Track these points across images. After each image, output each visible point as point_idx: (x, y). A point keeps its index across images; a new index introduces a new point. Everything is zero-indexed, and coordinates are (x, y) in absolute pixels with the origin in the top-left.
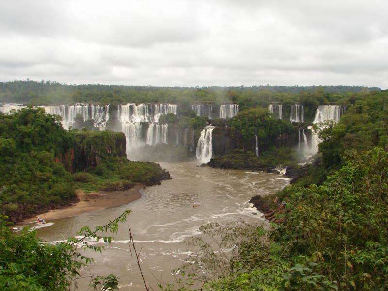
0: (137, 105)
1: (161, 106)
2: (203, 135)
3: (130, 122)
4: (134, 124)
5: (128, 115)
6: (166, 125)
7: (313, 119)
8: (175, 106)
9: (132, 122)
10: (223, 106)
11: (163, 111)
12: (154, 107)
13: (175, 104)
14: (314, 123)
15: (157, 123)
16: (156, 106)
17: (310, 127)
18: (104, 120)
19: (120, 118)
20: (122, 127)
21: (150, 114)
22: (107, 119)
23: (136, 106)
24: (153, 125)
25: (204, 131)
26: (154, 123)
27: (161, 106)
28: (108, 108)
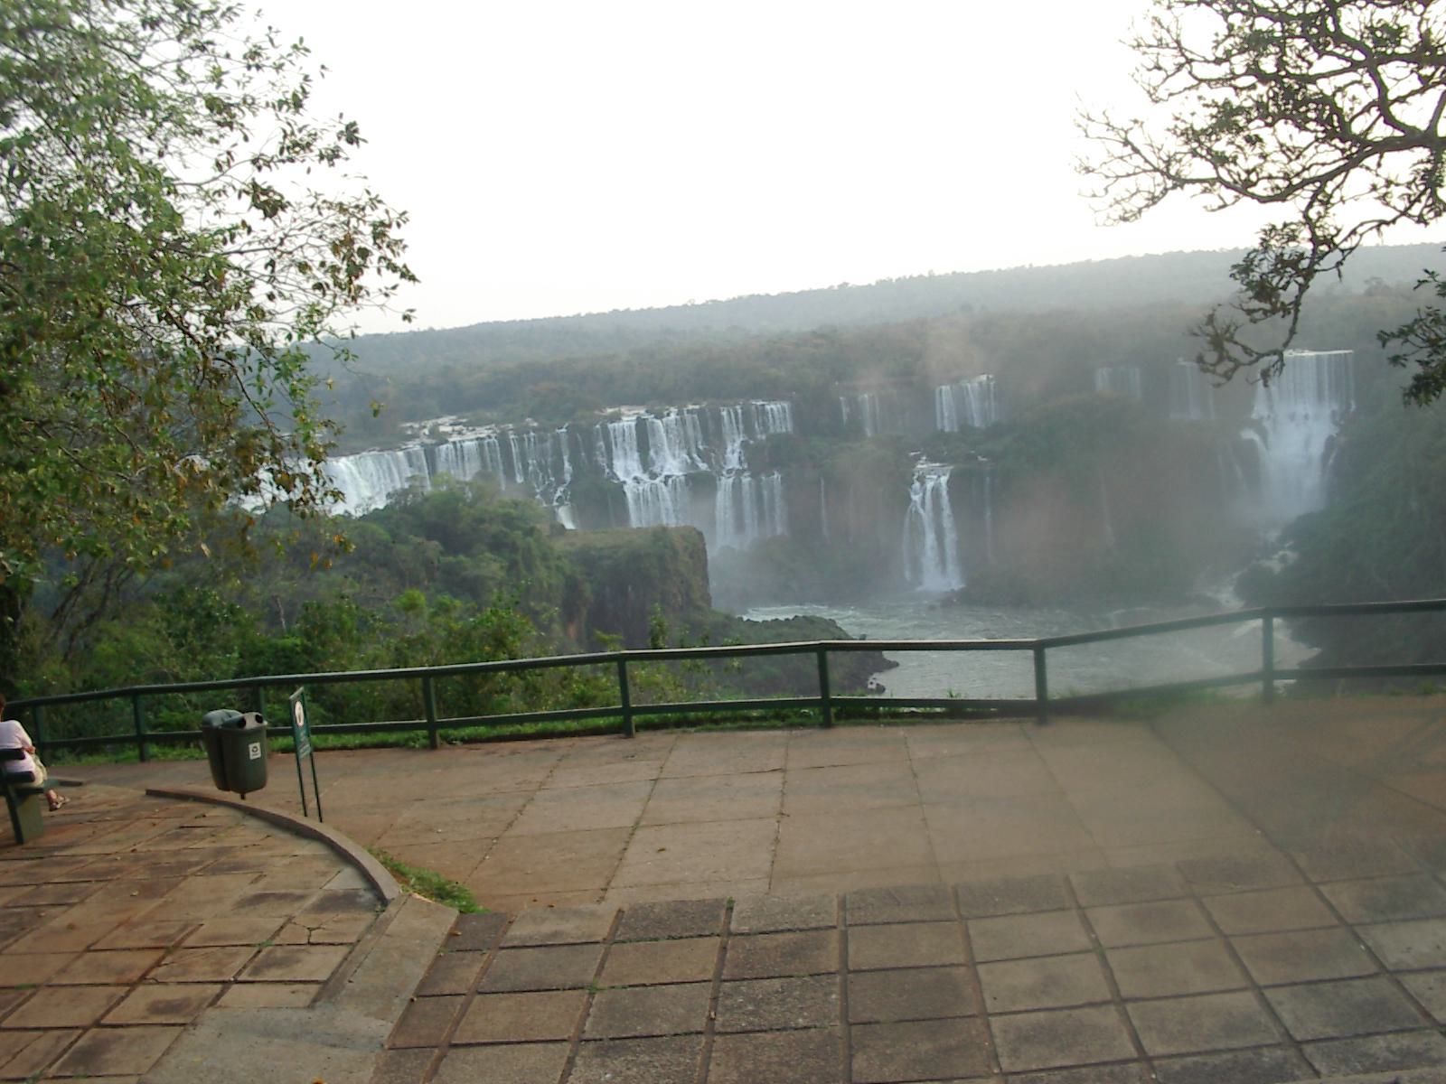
0: (659, 416)
1: (740, 411)
2: (916, 498)
3: (645, 477)
4: (666, 483)
5: (636, 455)
6: (777, 476)
7: (1250, 408)
8: (786, 405)
9: (653, 476)
10: (943, 387)
11: (749, 430)
12: (718, 420)
13: (783, 399)
14: (1254, 416)
15: (740, 472)
16: (724, 413)
17: (1249, 435)
18: (560, 481)
19: (611, 466)
20: (624, 493)
21: (706, 440)
22: (568, 478)
23: (658, 421)
24: (731, 480)
25: (917, 485)
26: (729, 471)
27: (740, 411)
28: (564, 439)
